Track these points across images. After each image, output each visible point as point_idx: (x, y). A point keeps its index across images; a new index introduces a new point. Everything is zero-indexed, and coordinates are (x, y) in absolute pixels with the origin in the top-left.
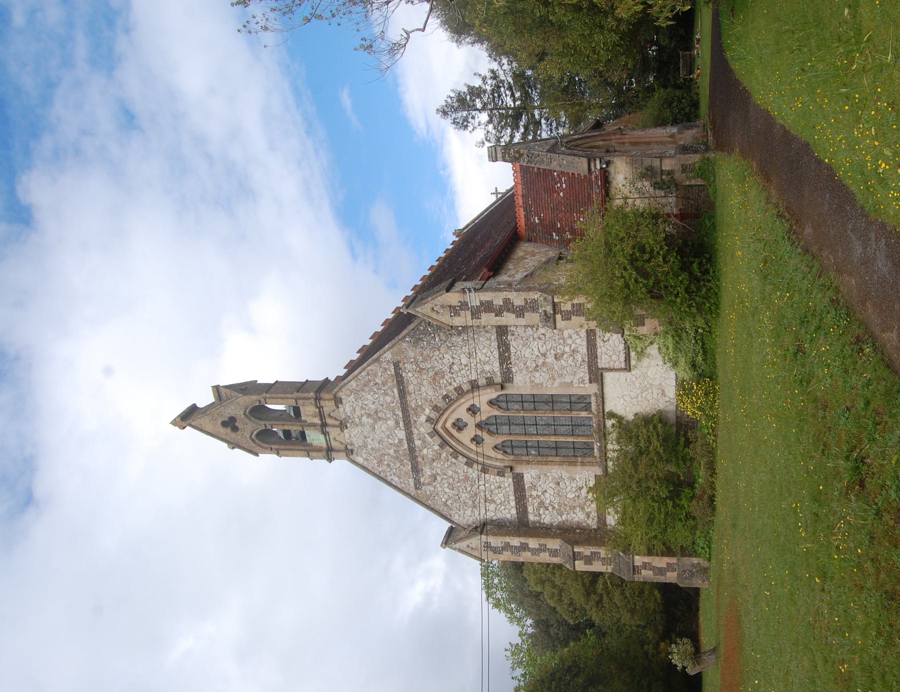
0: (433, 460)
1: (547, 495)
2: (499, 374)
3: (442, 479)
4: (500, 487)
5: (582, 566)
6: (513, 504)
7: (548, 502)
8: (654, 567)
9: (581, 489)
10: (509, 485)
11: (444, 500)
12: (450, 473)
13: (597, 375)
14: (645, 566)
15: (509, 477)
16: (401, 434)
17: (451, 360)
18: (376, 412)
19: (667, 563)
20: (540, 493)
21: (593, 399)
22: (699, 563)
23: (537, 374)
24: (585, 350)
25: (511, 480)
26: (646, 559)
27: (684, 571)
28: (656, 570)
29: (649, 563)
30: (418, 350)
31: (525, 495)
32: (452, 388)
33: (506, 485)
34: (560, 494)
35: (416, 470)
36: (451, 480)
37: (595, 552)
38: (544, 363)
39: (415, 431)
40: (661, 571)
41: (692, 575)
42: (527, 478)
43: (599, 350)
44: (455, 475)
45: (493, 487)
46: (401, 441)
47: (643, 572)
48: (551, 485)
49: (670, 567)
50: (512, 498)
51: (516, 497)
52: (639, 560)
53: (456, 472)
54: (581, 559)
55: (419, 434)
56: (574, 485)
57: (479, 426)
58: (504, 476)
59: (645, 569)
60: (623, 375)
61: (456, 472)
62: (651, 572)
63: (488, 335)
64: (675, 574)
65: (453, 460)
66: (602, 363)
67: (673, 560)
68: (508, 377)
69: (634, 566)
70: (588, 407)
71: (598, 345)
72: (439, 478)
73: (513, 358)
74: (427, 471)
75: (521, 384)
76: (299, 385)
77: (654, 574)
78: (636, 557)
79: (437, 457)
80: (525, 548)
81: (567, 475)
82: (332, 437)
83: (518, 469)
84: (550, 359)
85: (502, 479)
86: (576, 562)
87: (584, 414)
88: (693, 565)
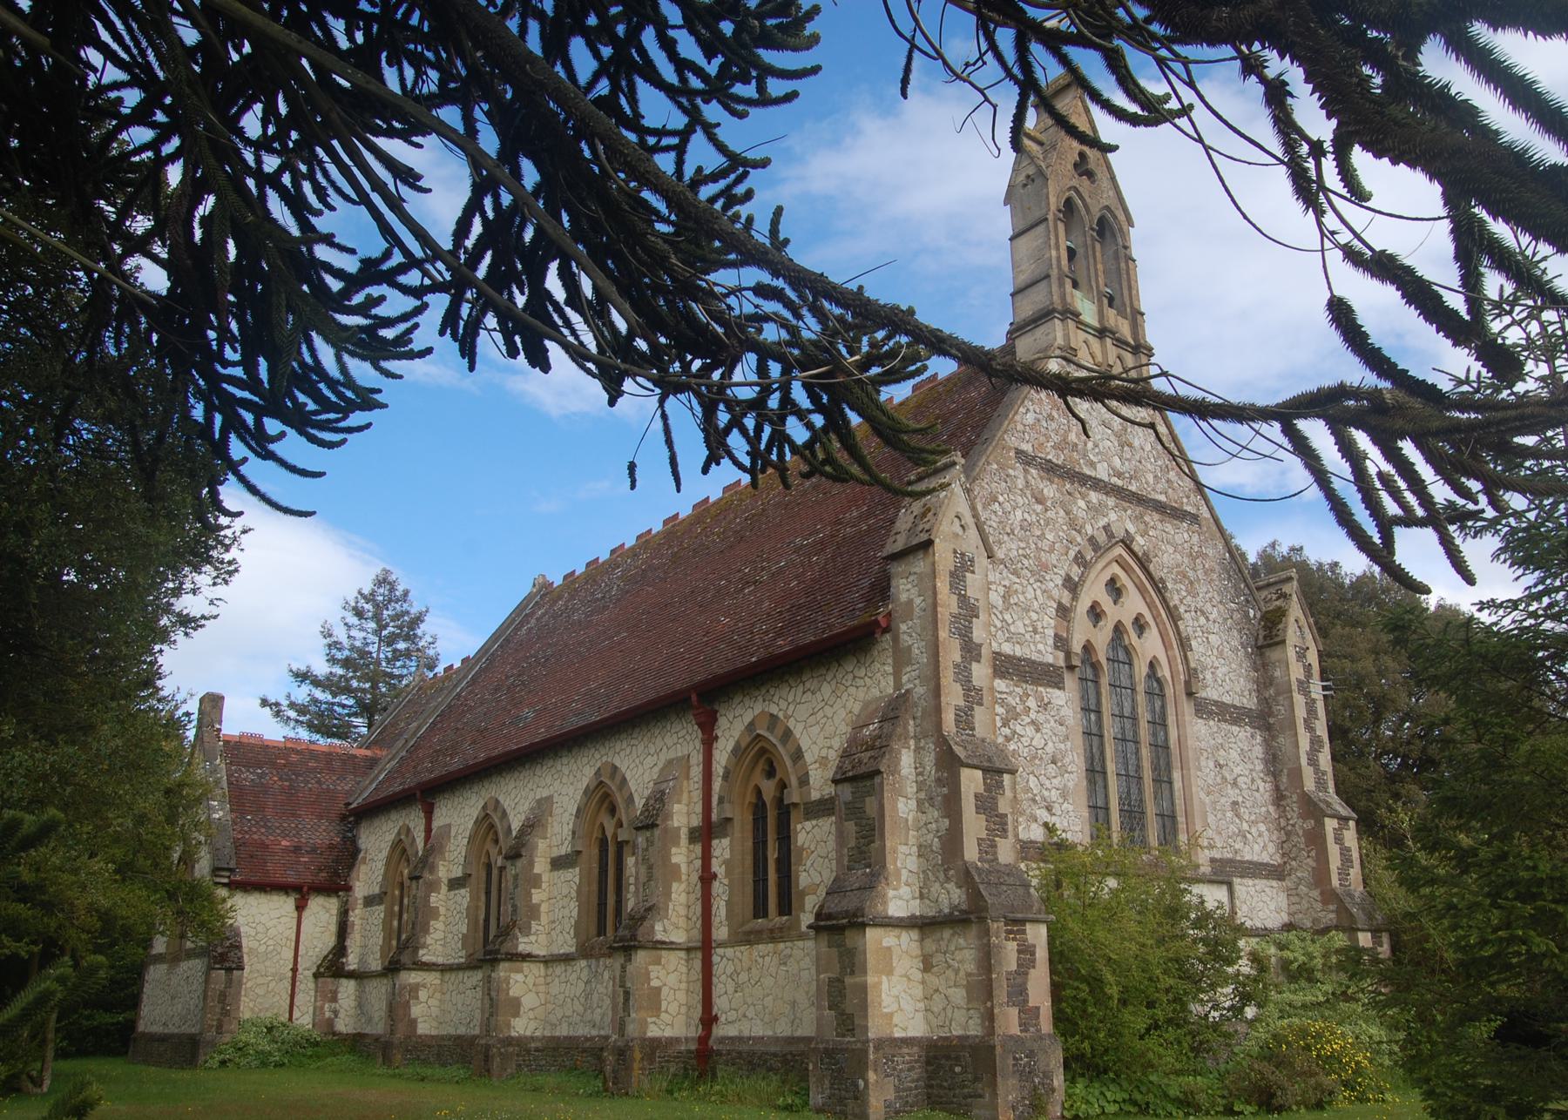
0: (1067, 513)
1: (1030, 731)
3: (1037, 514)
4: (1035, 631)
5: (973, 785)
7: (1019, 729)
8: (1027, 974)
9: (1049, 809)
10: (1039, 652)
11: (1001, 499)
12: (1050, 537)
14: (1026, 951)
15: (1056, 658)
16: (1102, 472)
17: (1211, 617)
18: (1130, 445)
19: (1038, 1008)
20: (1033, 715)
22: (1053, 1090)
24: (1247, 857)
25: (1050, 659)
26: (1042, 954)
27: (1031, 1054)
28: (1019, 980)
29: (1034, 961)
30: (1217, 568)
31: (1027, 682)
32: (1177, 602)
33: (1040, 647)
34: (1037, 761)
35: (1050, 469)
36: (1039, 533)
37: (1006, 824)
39: (1111, 502)
40: (1019, 993)
41: (1025, 1074)
42: (1058, 697)
43: (1250, 882)
44: (1045, 545)
45: (1034, 616)
46: (1092, 465)
47: (1012, 946)
48: (1050, 744)
49: (1029, 1016)
50: (1018, 651)
51: (1020, 659)
52: (1038, 935)
53: (1052, 550)
54: (988, 788)
55: (1106, 506)
56: (1054, 795)
58: (1056, 647)
59: (1019, 952)
61: (1052, 550)
62: (1014, 967)
63: (1246, 693)
64: (1015, 1030)
65: (1072, 554)
67: (1046, 1024)
69: (1023, 922)
71: (1257, 881)
72: (1039, 508)
73: (1224, 725)
74: (1050, 491)
77: (1009, 973)
78: (1043, 930)
79: (1073, 524)
80: (969, 651)
81: (1071, 784)
82: (1090, 338)
83: (1070, 681)
84: (1233, 794)
85: (1051, 641)
86: (979, 773)
88: (1048, 1075)
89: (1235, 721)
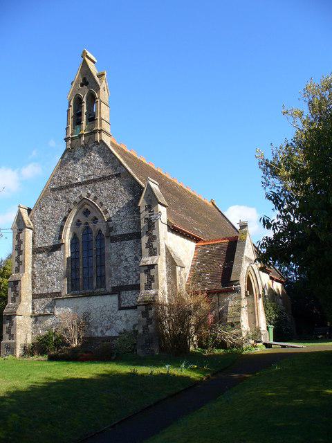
2: (115, 234)
6: (44, 245)
13: (117, 291)
21: (102, 290)
23: (115, 256)
38: (122, 261)
57: (87, 223)
60: (116, 306)
66: (123, 293)
68: (114, 239)
70: (97, 287)
75: (111, 248)
76: (90, 97)
84: (125, 264)
87: (95, 284)
89: (129, 239)
